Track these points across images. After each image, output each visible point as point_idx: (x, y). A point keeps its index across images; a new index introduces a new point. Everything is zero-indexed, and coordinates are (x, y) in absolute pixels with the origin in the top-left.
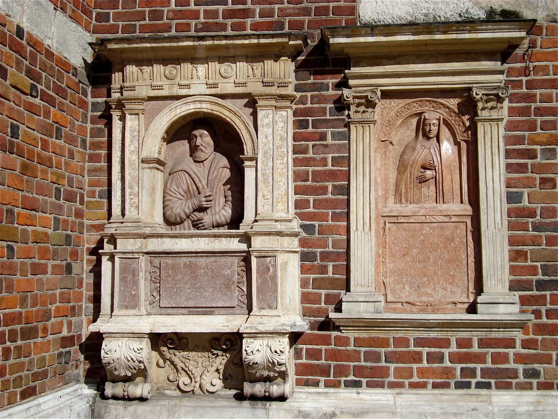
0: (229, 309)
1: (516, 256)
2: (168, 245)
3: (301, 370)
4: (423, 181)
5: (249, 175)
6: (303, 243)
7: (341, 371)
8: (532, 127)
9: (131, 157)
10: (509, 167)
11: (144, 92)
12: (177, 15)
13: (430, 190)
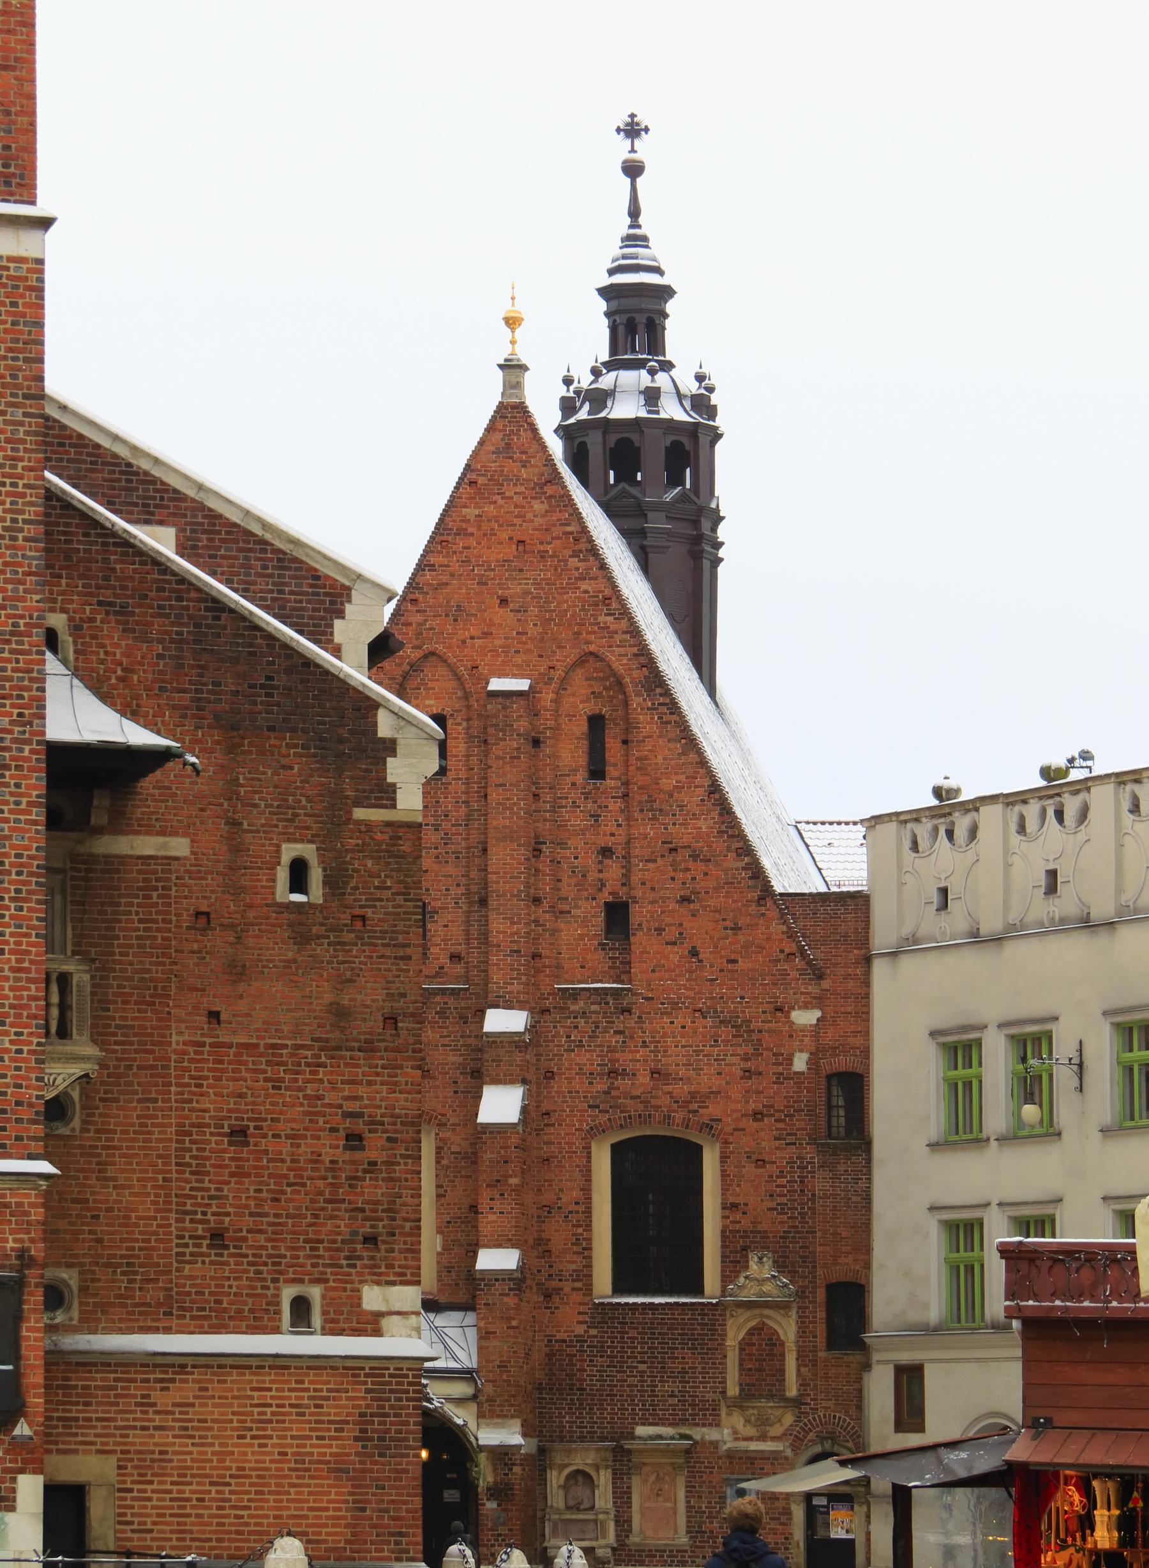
0: (591, 1540)
1: (689, 1522)
2: (568, 1517)
3: (615, 1560)
4: (658, 1495)
5: (597, 1492)
6: (615, 1516)
7: (630, 1561)
8: (695, 1477)
9: (555, 1485)
10: (687, 1492)
11: (559, 1462)
12: (569, 1432)
13: (661, 1499)
